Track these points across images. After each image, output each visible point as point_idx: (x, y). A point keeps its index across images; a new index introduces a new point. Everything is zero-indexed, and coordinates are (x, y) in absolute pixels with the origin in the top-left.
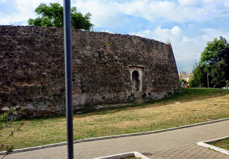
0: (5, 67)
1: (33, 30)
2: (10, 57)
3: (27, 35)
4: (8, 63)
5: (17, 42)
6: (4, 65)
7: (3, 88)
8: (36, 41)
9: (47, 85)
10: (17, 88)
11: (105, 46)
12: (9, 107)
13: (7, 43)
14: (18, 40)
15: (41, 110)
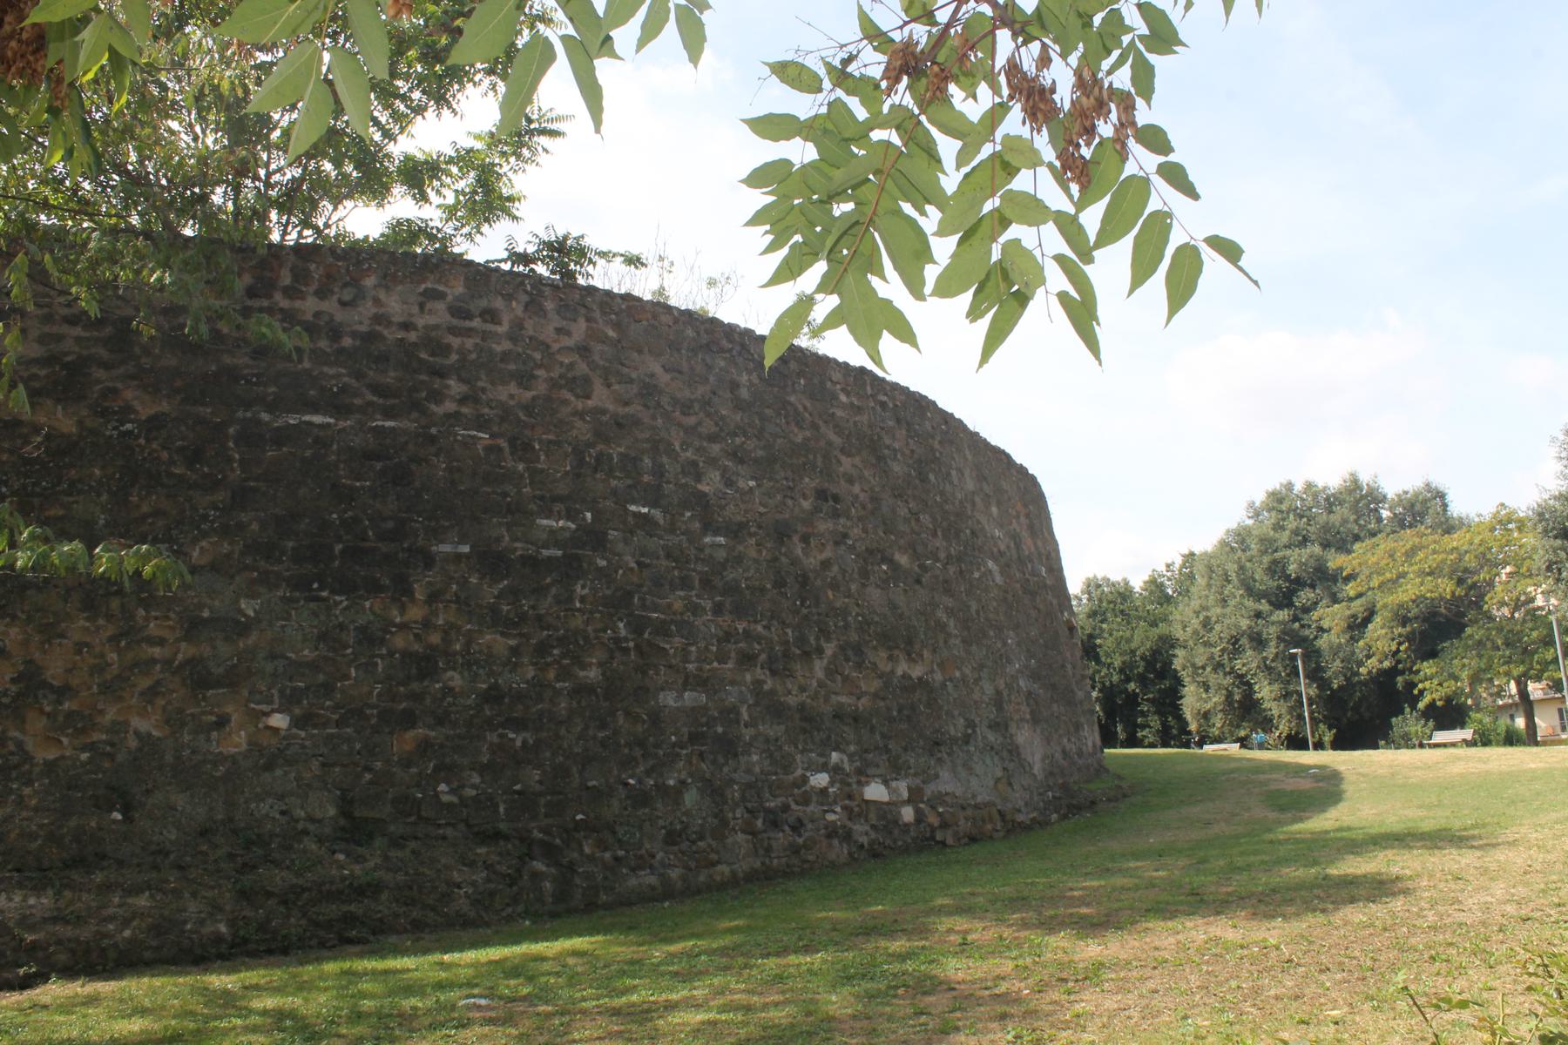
0: (826, 564)
1: (869, 391)
2: (836, 515)
3: (859, 410)
4: (837, 543)
5: (837, 440)
6: (821, 552)
7: (846, 679)
8: (888, 447)
9: (958, 674)
10: (887, 677)
11: (1018, 517)
12: (886, 783)
13: (808, 434)
14: (838, 429)
15: (979, 799)
